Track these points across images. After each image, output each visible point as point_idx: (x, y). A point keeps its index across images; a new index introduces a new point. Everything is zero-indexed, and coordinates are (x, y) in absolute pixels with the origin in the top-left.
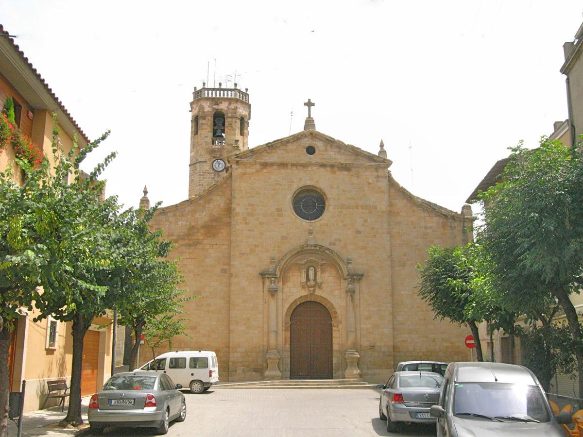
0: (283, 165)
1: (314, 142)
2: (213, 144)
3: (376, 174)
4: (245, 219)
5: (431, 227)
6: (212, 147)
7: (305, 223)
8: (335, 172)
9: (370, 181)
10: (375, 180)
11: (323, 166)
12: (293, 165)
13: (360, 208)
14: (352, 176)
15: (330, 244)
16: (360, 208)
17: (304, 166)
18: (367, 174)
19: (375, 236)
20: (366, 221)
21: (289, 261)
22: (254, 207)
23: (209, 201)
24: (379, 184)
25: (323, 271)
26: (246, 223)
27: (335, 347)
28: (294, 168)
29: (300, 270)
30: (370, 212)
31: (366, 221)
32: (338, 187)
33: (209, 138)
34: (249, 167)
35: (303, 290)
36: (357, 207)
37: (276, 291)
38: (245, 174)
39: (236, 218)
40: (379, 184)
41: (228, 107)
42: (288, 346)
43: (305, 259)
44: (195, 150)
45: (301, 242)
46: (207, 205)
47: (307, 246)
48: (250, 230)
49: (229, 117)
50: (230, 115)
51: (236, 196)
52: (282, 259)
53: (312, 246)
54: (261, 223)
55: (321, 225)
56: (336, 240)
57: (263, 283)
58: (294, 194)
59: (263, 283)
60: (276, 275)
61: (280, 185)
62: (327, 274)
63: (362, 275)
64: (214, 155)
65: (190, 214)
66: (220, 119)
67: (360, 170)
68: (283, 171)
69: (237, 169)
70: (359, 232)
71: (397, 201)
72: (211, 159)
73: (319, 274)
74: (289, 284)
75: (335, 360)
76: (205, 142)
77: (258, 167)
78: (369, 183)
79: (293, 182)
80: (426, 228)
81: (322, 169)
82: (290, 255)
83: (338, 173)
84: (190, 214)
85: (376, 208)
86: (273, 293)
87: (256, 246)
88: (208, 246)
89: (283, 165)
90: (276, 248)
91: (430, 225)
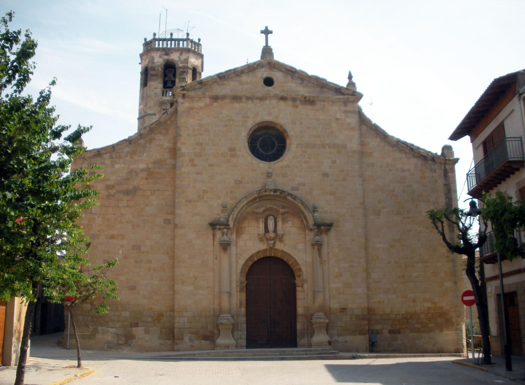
0: (236, 98)
1: (273, 73)
2: (163, 95)
3: (343, 108)
4: (192, 160)
5: (408, 170)
6: (161, 98)
7: (264, 165)
8: (297, 107)
9: (338, 116)
10: (343, 114)
11: (283, 99)
12: (248, 98)
13: (327, 147)
14: (317, 110)
15: (293, 188)
16: (327, 147)
17: (262, 99)
18: (335, 108)
19: (345, 180)
20: (334, 162)
21: (244, 208)
22: (203, 146)
23: (151, 141)
24: (348, 120)
25: (284, 221)
26: (194, 165)
27: (300, 310)
28: (250, 102)
29: (257, 220)
30: (339, 152)
31: (334, 162)
32: (301, 124)
33: (158, 89)
34: (197, 101)
35: (261, 244)
36: (323, 146)
37: (229, 244)
38: (192, 108)
39: (181, 159)
40: (348, 120)
41: (179, 57)
42: (243, 310)
43: (263, 206)
44: (144, 102)
45: (258, 187)
46: (148, 145)
47: (266, 191)
48: (197, 173)
49: (180, 68)
50: (181, 65)
51: (182, 134)
52: (236, 207)
53: (271, 190)
54: (211, 165)
55: (282, 167)
56: (299, 184)
57: (214, 235)
58: (250, 131)
59: (214, 235)
60: (228, 225)
61: (233, 120)
62: (289, 224)
63: (329, 226)
64: (163, 107)
65: (129, 156)
66: (171, 69)
67: (326, 104)
68: (236, 105)
69: (183, 103)
70: (326, 175)
71: (369, 140)
72: (160, 111)
73: (280, 224)
74: (244, 237)
75: (299, 326)
76: (155, 93)
77: (208, 100)
78: (337, 119)
79: (248, 117)
80: (403, 171)
81: (282, 103)
82: (245, 202)
83: (301, 107)
84: (129, 156)
85: (345, 147)
86: (225, 246)
87: (205, 192)
88: (149, 193)
89: (236, 98)
90: (229, 194)
91: (406, 167)
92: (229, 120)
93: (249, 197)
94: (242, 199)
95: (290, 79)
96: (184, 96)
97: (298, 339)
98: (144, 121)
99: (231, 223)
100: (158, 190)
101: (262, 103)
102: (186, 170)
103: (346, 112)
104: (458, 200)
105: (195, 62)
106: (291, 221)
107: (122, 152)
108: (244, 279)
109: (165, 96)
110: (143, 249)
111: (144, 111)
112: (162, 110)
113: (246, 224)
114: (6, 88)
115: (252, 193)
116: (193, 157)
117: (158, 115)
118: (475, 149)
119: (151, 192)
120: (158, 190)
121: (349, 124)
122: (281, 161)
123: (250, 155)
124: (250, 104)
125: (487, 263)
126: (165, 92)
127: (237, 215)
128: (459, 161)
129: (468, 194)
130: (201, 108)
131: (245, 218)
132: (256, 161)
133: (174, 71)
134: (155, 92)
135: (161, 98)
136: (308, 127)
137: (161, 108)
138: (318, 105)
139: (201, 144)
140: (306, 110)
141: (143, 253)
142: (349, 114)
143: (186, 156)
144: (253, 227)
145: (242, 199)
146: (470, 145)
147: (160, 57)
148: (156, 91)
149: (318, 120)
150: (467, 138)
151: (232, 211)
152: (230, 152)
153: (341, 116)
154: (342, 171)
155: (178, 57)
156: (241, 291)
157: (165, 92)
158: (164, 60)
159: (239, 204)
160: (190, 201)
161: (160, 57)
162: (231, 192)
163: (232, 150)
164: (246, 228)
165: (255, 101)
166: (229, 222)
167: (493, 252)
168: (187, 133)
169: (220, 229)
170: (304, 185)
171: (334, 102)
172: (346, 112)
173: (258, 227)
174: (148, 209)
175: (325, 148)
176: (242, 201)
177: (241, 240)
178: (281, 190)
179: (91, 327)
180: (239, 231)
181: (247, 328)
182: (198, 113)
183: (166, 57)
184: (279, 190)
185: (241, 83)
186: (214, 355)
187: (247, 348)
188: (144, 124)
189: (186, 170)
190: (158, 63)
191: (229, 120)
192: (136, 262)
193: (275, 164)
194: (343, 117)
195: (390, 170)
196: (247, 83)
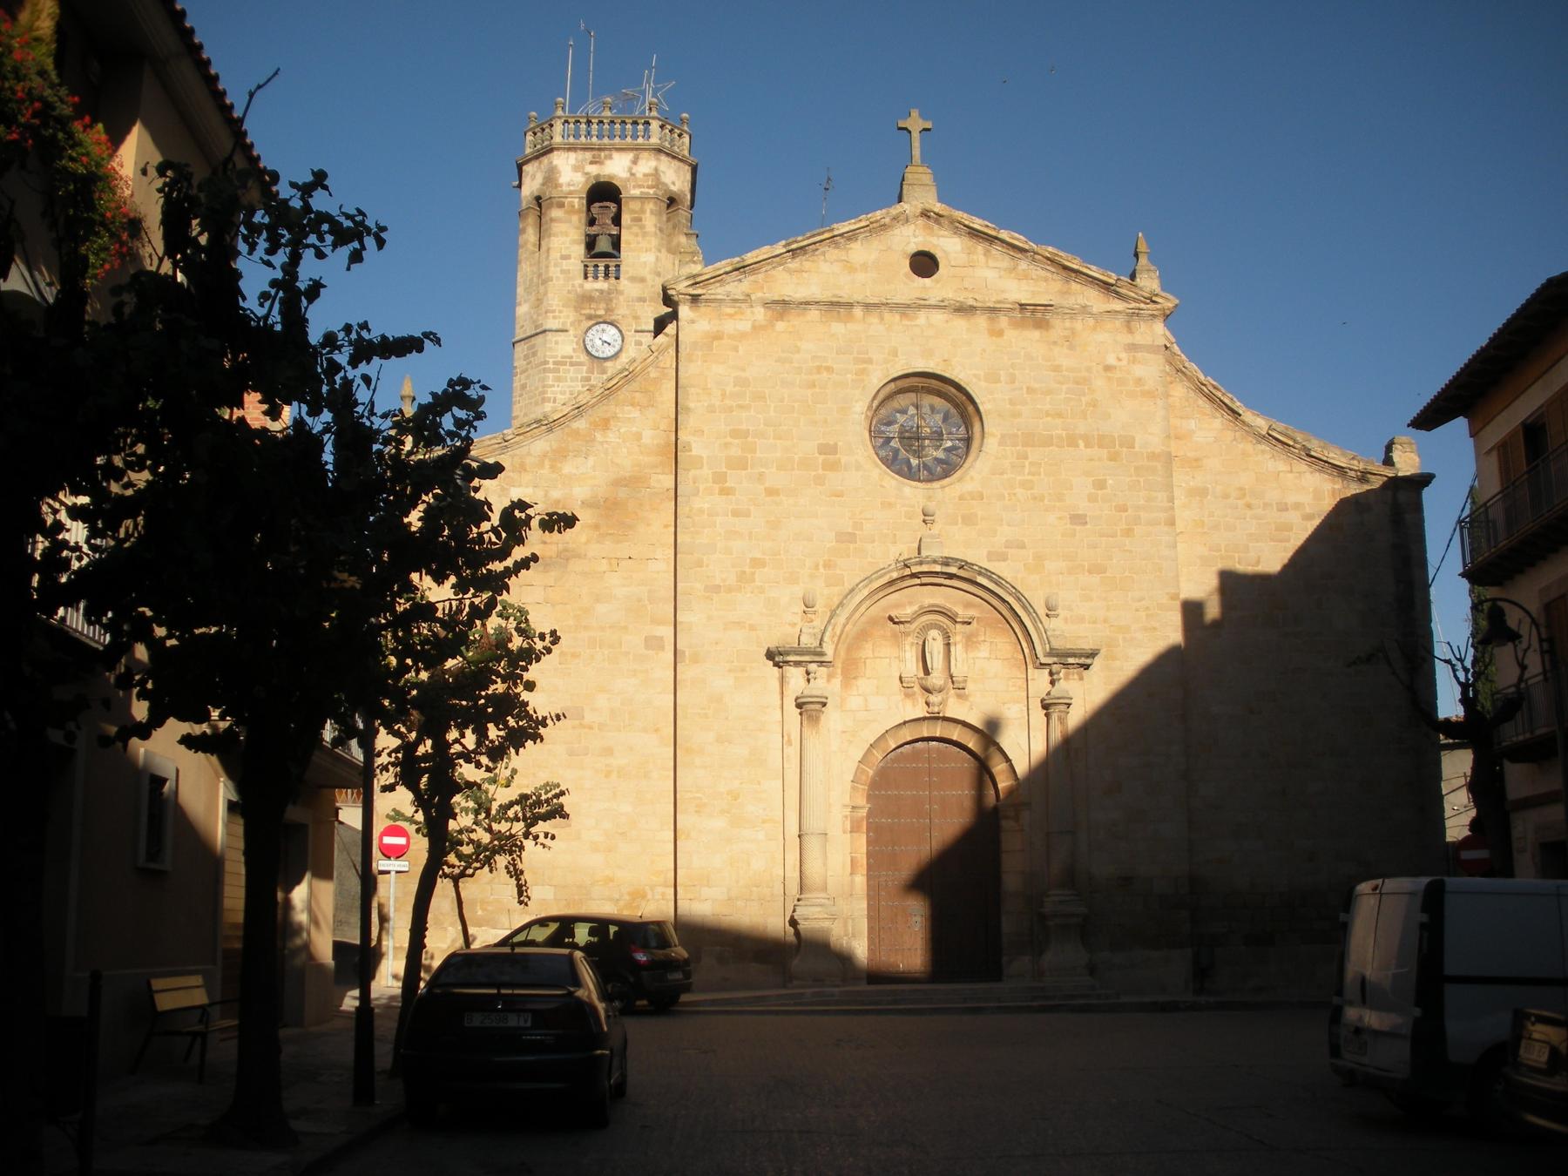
0: (836, 307)
1: (934, 240)
2: (586, 277)
3: (1126, 338)
4: (719, 478)
5: (1297, 506)
6: (581, 286)
7: (914, 493)
8: (1000, 333)
9: (1111, 360)
10: (1123, 355)
11: (963, 310)
12: (868, 306)
13: (1081, 443)
14: (1055, 343)
15: (991, 556)
16: (1081, 443)
17: (906, 309)
18: (1102, 336)
19: (1128, 532)
20: (1101, 485)
21: (863, 609)
22: (750, 439)
23: (605, 424)
24: (1139, 371)
25: (970, 641)
26: (726, 492)
27: (1011, 881)
28: (874, 319)
29: (897, 640)
30: (1114, 457)
31: (1101, 485)
32: (1012, 380)
33: (572, 260)
34: (731, 316)
35: (909, 703)
36: (1072, 441)
37: (824, 705)
38: (718, 336)
39: (692, 473)
40: (1139, 371)
41: (630, 170)
42: (861, 880)
43: (911, 603)
44: (533, 298)
45: (906, 550)
46: (599, 436)
47: (921, 563)
48: (736, 513)
49: (634, 198)
50: (636, 192)
51: (692, 405)
52: (841, 604)
53: (935, 562)
54: (771, 492)
55: (961, 498)
56: (1008, 545)
57: (782, 680)
58: (874, 398)
59: (782, 680)
60: (822, 654)
61: (829, 369)
62: (983, 652)
63: (1093, 654)
64: (587, 311)
65: (547, 463)
66: (608, 204)
67: (1078, 325)
68: (838, 328)
69: (693, 322)
70: (1078, 519)
71: (1192, 424)
72: (580, 321)
73: (957, 651)
74: (863, 684)
75: (1008, 925)
76: (562, 271)
77: (760, 313)
78: (1108, 368)
79: (870, 361)
80: (1283, 508)
81: (960, 323)
82: (866, 592)
83: (1011, 334)
84: (547, 463)
85: (1129, 443)
86: (809, 708)
87: (757, 563)
88: (604, 565)
89: (836, 307)
90: (822, 570)
91: (1292, 499)
92: (819, 369)
93: (877, 579)
94: (857, 585)
95: (982, 258)
96: (695, 299)
97: (1005, 959)
98: (533, 350)
99: (829, 649)
100: (630, 558)
101: (906, 322)
102: (706, 506)
103: (1132, 348)
104: (1430, 586)
105: (674, 183)
106: (987, 644)
107: (529, 454)
108: (861, 801)
109: (590, 279)
110: (589, 717)
111: (534, 322)
112: (584, 318)
113: (867, 651)
114: (347, 324)
115: (884, 568)
116: (725, 470)
117: (571, 332)
118: (1480, 455)
119: (610, 564)
120: (630, 558)
121: (1139, 381)
122: (960, 479)
123: (877, 466)
124: (874, 325)
125: (1514, 760)
126: (591, 269)
127: (845, 626)
128: (1434, 481)
129: (1463, 577)
130: (743, 336)
131: (863, 636)
132: (891, 481)
133: (614, 210)
134: (564, 268)
135: (581, 286)
136: (1030, 390)
137: (581, 314)
138: (1059, 326)
139: (746, 434)
140: (1025, 341)
141: (591, 728)
142: (1139, 355)
143: (705, 467)
144: (887, 658)
145: (857, 585)
146: (1469, 443)
147: (576, 168)
148: (565, 264)
149: (1057, 369)
150: (1460, 424)
151: (831, 617)
152: (823, 457)
153: (1119, 360)
154: (1123, 509)
155: (626, 169)
156: (854, 829)
157: (591, 269)
158: (587, 180)
159: (849, 597)
160: (716, 589)
161: (576, 168)
162: (827, 565)
163: (828, 449)
164: (868, 661)
165: (887, 316)
166: (824, 645)
167: (1532, 732)
168: (706, 404)
169: (798, 664)
170: (1023, 546)
171: (1099, 318)
172: (1132, 348)
173: (901, 660)
174: (601, 608)
175: (1077, 446)
176: (857, 590)
177: (855, 693)
178: (962, 561)
179: (450, 928)
180: (851, 671)
181: (871, 930)
182: (736, 349)
183: (593, 170)
184: (957, 560)
185: (851, 268)
186: (792, 1002)
187: (869, 983)
188: (532, 359)
189: (706, 506)
190: (569, 185)
191: (819, 369)
192: (571, 753)
193: (943, 487)
194: (1124, 363)
195: (1249, 506)
196: (865, 267)
